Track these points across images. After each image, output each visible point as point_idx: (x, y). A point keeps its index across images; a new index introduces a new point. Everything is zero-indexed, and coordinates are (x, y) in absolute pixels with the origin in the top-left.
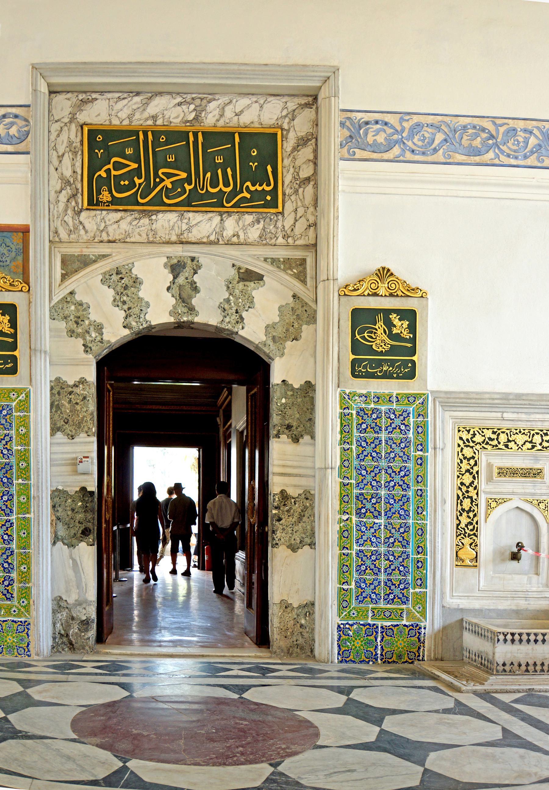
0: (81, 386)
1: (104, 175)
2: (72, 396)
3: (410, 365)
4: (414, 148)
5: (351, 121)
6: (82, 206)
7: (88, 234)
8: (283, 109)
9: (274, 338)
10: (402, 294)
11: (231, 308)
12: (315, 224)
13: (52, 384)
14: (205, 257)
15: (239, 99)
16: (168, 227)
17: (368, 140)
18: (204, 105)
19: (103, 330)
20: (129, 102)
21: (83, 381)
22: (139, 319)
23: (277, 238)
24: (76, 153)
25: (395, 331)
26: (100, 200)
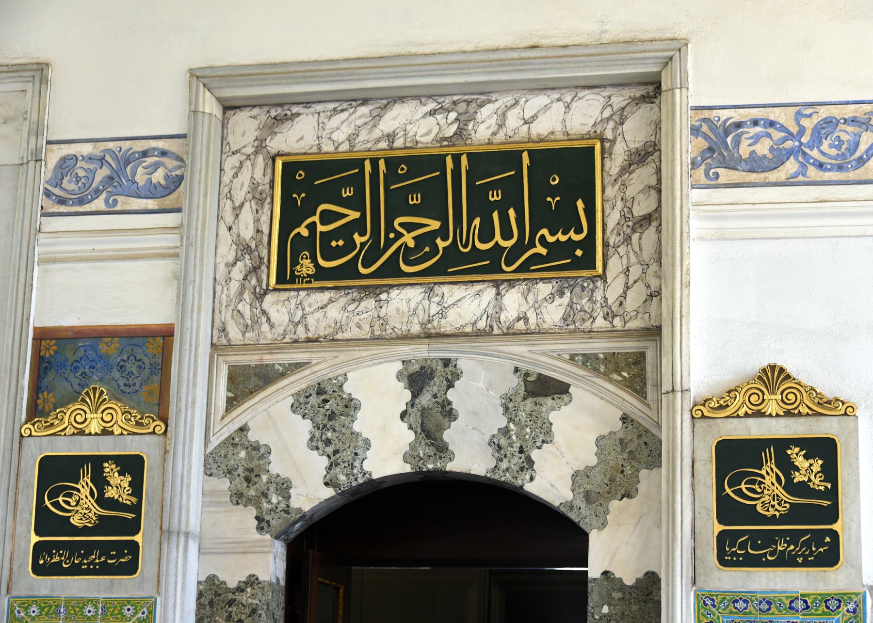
0: (249, 590)
1: (305, 233)
2: (234, 609)
3: (828, 539)
4: (822, 159)
5: (711, 124)
6: (268, 285)
7: (274, 331)
8: (604, 108)
9: (588, 497)
10: (807, 410)
11: (511, 445)
12: (659, 293)
13: (201, 587)
14: (467, 359)
15: (531, 97)
16: (406, 309)
17: (741, 152)
18: (473, 110)
19: (291, 491)
20: (350, 115)
21: (252, 581)
22: (352, 469)
23: (594, 319)
24: (261, 201)
25: (798, 478)
26: (297, 274)
